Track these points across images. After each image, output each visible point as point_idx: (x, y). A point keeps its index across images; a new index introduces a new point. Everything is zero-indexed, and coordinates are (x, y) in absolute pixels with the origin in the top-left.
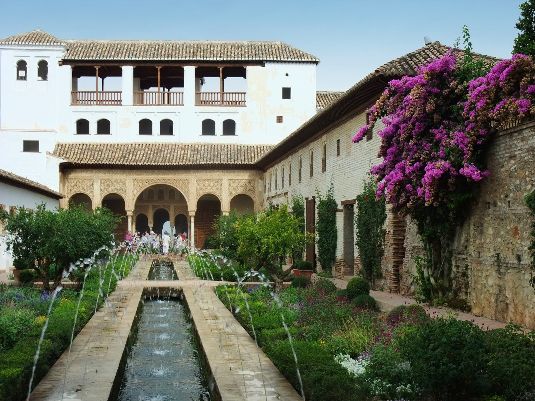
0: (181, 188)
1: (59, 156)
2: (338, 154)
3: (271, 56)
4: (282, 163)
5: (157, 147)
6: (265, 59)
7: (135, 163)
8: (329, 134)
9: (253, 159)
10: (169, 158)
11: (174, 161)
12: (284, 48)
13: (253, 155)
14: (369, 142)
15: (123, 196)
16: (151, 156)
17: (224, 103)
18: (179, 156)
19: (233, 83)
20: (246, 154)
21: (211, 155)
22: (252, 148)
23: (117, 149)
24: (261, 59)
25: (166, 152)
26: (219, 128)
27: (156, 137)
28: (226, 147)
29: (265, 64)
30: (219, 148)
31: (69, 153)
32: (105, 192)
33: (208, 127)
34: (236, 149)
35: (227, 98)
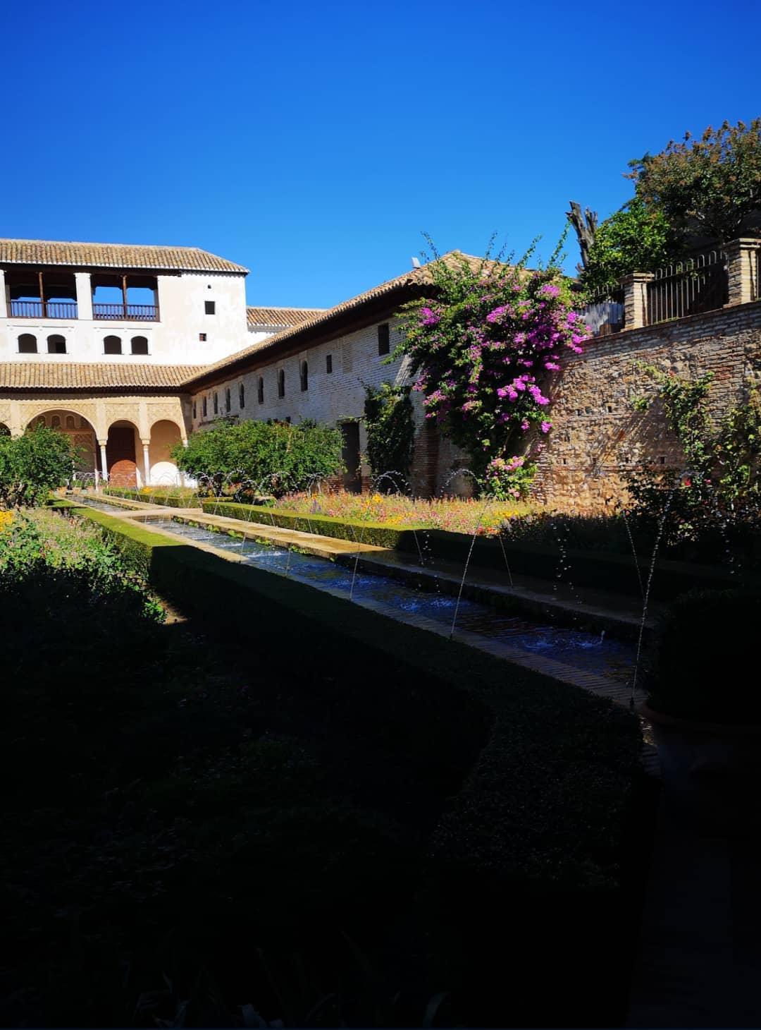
0: (86, 414)
2: (329, 370)
3: (189, 265)
4: (226, 384)
6: (181, 268)
8: (312, 351)
9: (177, 381)
12: (202, 256)
13: (175, 377)
14: (383, 356)
17: (126, 317)
19: (138, 295)
20: (166, 376)
22: (172, 369)
24: (176, 268)
26: (126, 346)
28: (138, 368)
29: (180, 273)
35: (130, 311)
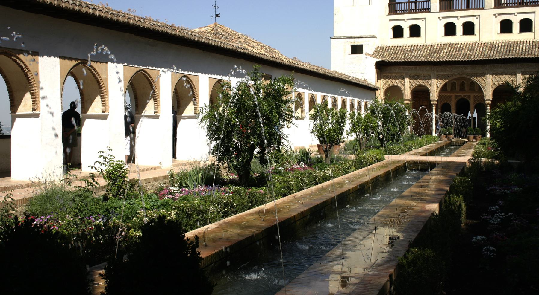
1: (375, 57)
5: (459, 46)
7: (438, 60)
10: (469, 54)
11: (473, 57)
15: (429, 87)
16: (453, 54)
18: (477, 53)
21: (506, 51)
23: (425, 49)
25: (466, 50)
27: (460, 38)
28: (522, 43)
30: (516, 44)
31: (385, 54)
32: (414, 84)
33: (506, 27)
34: (531, 44)
